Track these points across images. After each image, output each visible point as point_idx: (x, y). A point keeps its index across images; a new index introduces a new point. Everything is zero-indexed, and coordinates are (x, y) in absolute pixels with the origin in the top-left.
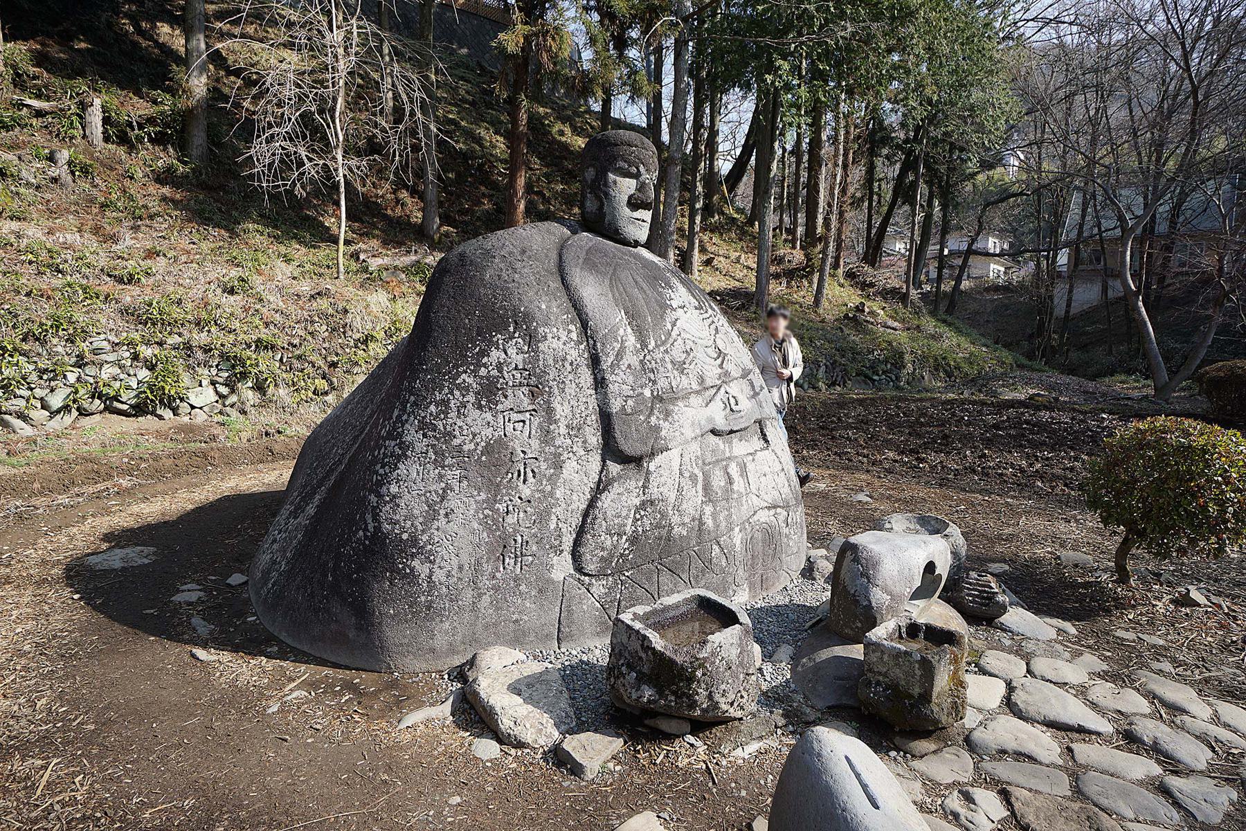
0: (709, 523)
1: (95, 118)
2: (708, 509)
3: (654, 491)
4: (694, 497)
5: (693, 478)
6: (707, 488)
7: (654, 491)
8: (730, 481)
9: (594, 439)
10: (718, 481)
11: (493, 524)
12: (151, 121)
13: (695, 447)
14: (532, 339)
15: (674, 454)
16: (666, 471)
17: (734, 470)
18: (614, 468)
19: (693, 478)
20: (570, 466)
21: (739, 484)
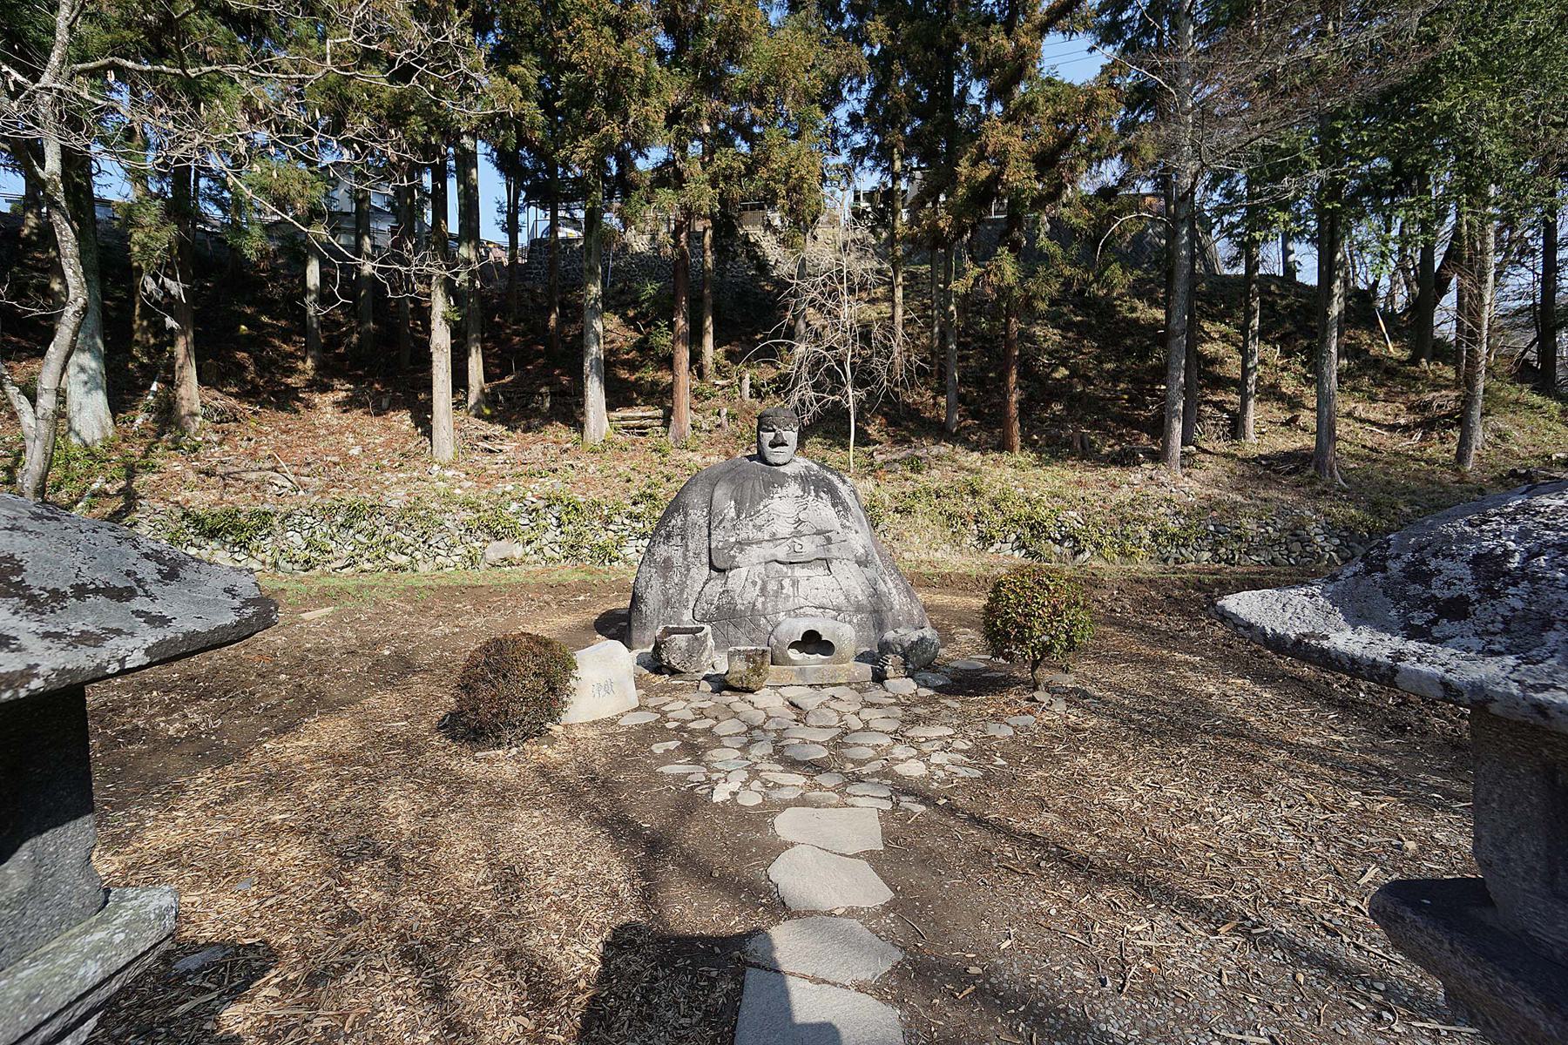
0: (759, 606)
1: (747, 382)
2: (761, 599)
3: (729, 586)
4: (752, 593)
5: (754, 583)
6: (763, 589)
7: (729, 586)
8: (782, 587)
9: (705, 560)
10: (772, 586)
11: (665, 592)
12: (774, 381)
13: (761, 569)
14: (686, 514)
15: (743, 571)
16: (736, 579)
17: (786, 583)
18: (714, 574)
19: (754, 583)
20: (694, 571)
21: (788, 590)
